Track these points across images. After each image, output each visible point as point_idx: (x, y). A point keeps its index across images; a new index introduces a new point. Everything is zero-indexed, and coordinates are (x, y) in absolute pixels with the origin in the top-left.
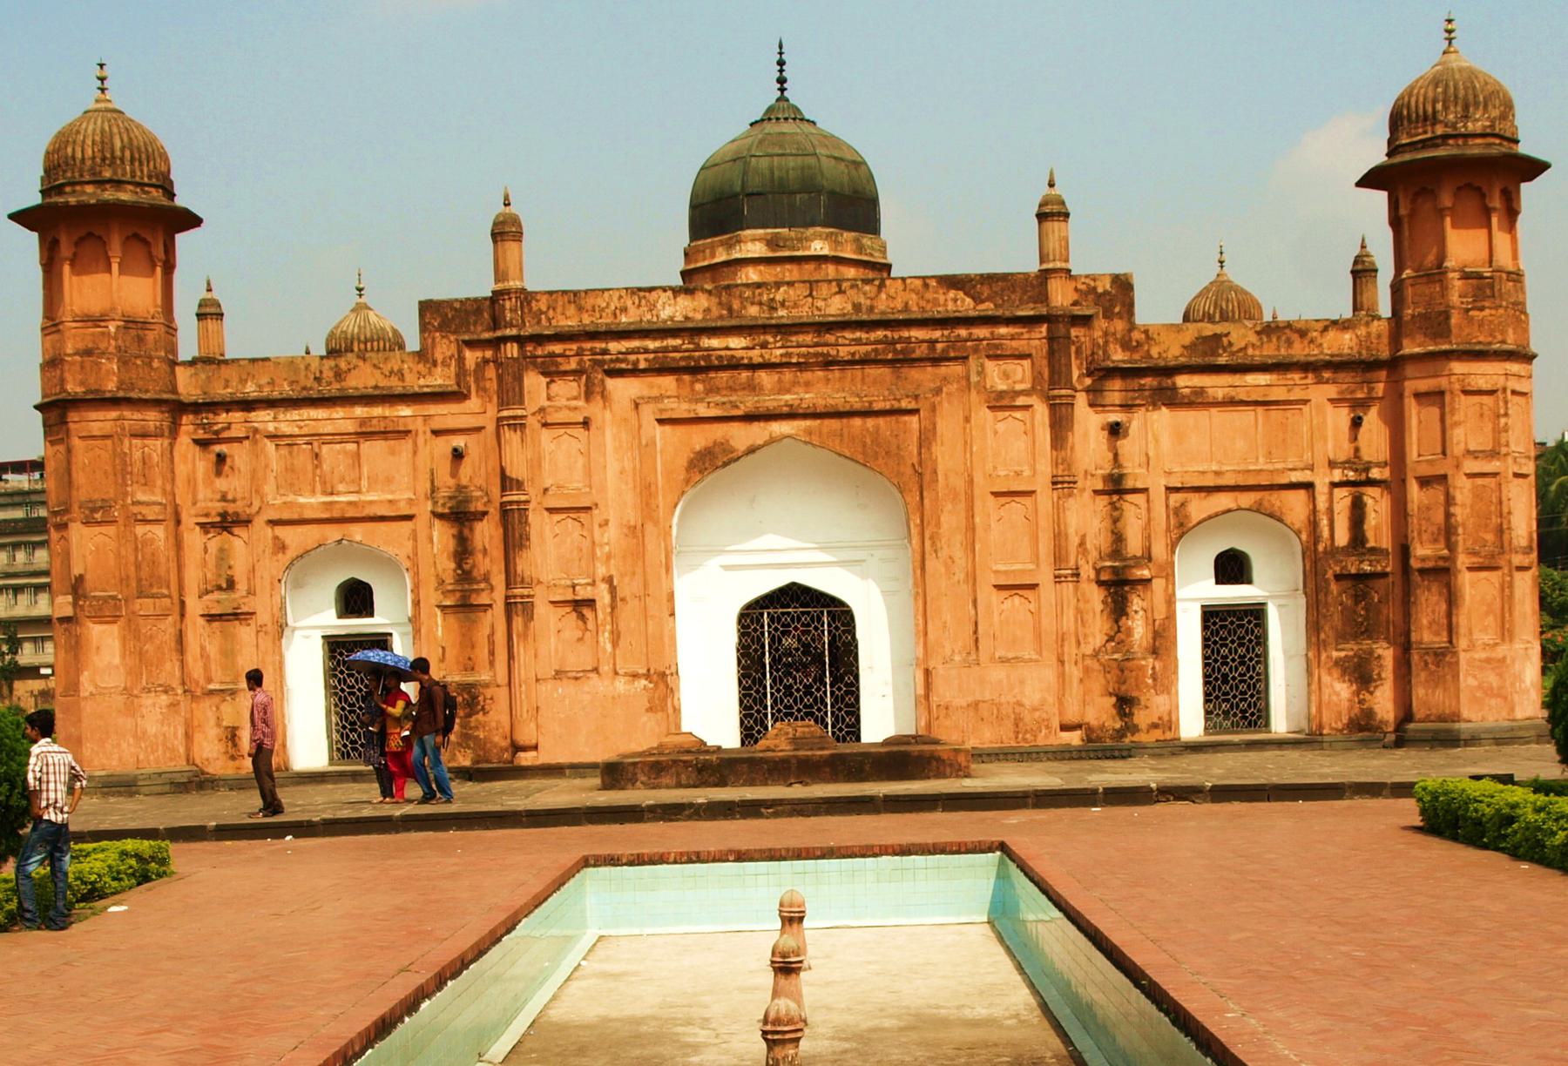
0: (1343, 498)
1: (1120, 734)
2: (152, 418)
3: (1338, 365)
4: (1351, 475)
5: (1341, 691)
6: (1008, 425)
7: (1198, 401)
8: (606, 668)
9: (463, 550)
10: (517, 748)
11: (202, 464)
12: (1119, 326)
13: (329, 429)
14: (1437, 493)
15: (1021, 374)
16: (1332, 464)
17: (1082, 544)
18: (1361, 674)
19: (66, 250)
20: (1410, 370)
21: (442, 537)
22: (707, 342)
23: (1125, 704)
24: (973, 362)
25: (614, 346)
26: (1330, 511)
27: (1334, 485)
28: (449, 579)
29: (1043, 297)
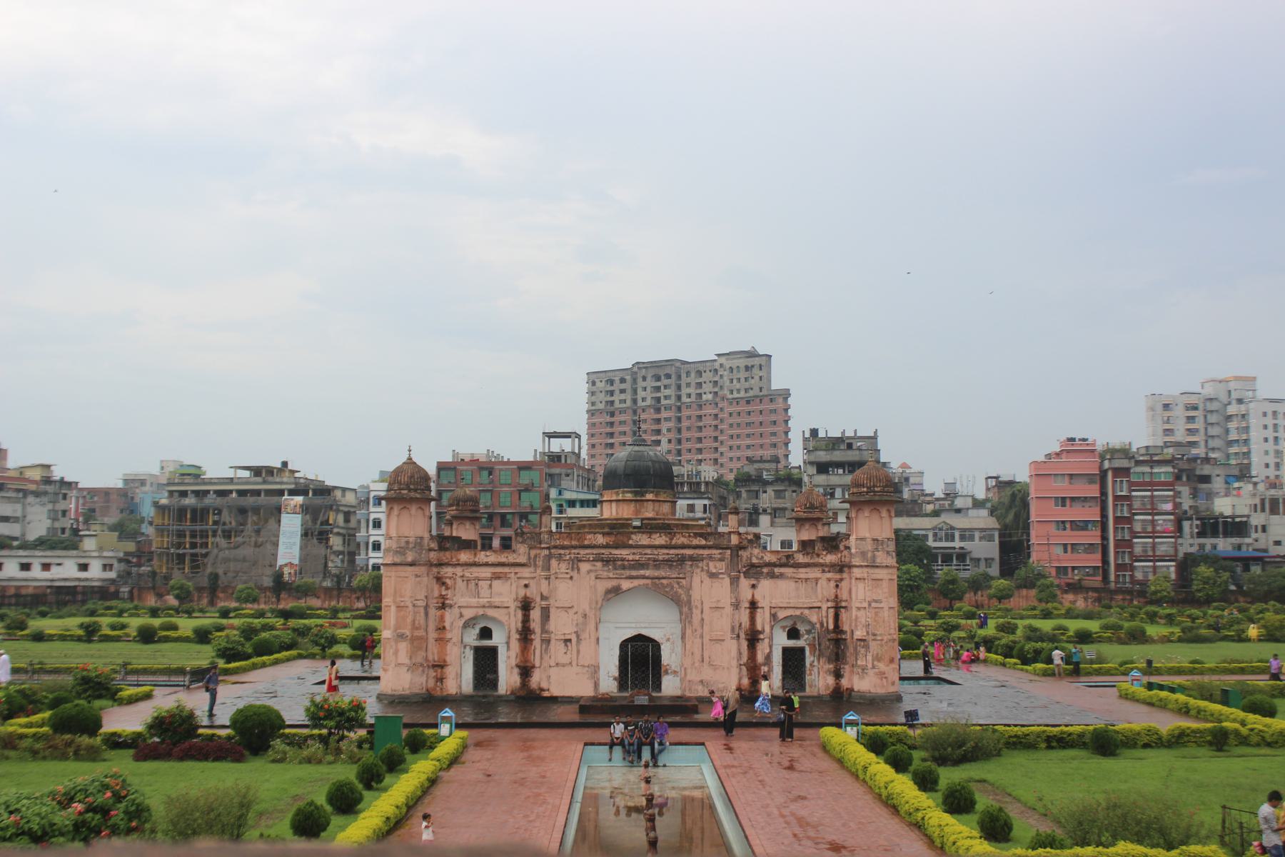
0: (832, 612)
5: (831, 680)
6: (716, 583)
7: (781, 576)
8: (574, 663)
9: (526, 620)
10: (542, 690)
12: (756, 551)
13: (483, 575)
14: (862, 612)
15: (721, 567)
18: (838, 675)
19: (396, 511)
20: (855, 570)
25: (583, 552)
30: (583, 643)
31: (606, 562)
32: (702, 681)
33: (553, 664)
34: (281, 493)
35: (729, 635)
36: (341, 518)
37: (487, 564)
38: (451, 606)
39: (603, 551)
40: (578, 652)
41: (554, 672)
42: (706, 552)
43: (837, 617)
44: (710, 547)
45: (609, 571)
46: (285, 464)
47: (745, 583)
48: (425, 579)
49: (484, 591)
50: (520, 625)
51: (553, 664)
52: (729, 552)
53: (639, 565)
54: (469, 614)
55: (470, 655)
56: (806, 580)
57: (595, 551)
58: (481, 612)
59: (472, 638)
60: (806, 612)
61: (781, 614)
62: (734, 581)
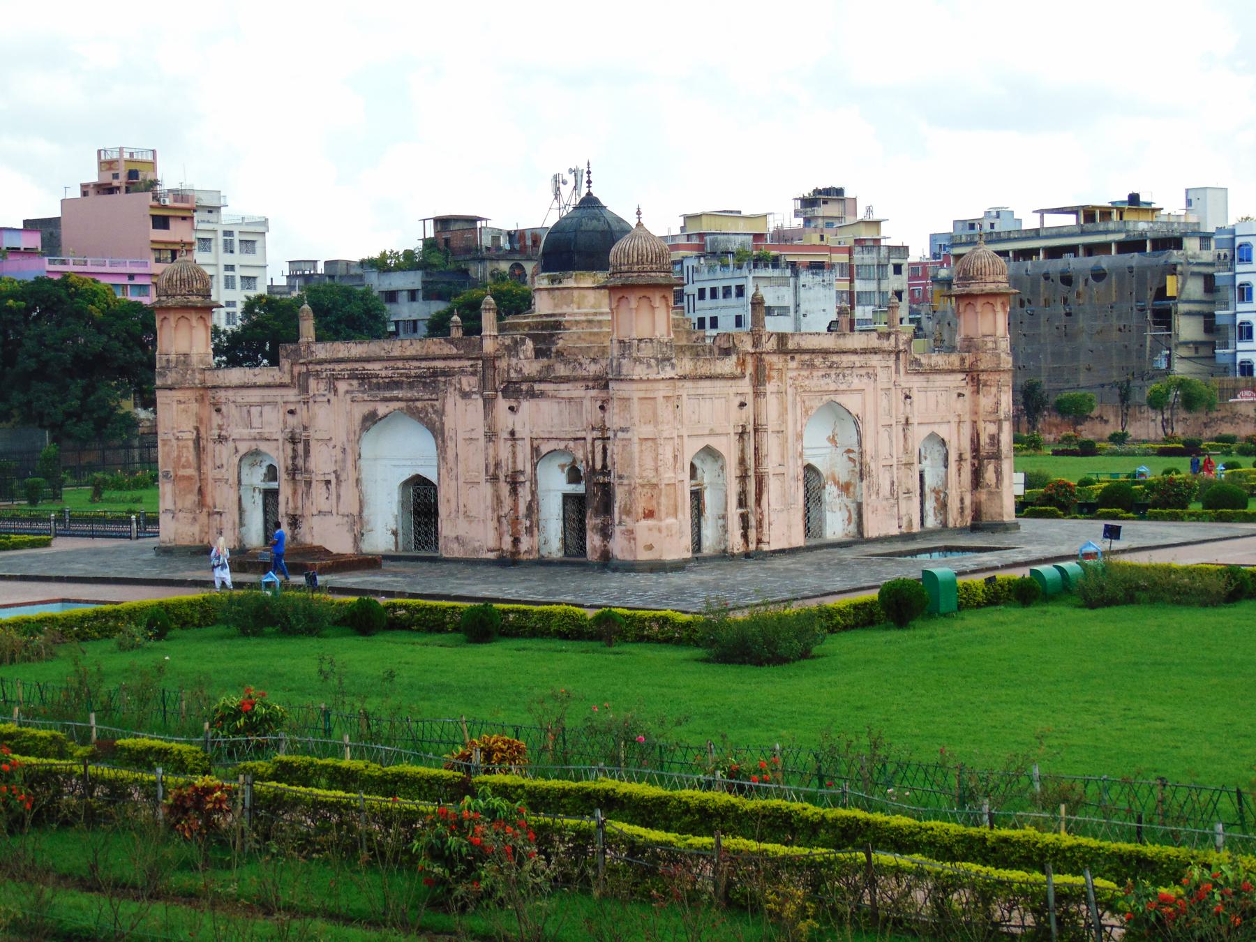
1: (513, 554)
2: (189, 393)
3: (596, 379)
4: (599, 434)
7: (542, 395)
11: (215, 413)
12: (514, 361)
13: (253, 399)
16: (593, 429)
17: (497, 465)
21: (289, 447)
22: (369, 366)
23: (516, 541)
24: (457, 377)
26: (593, 452)
27: (594, 440)
28: (291, 467)
29: (481, 348)
30: (343, 484)
31: (364, 378)
32: (457, 538)
33: (315, 512)
34: (1104, 248)
35: (483, 477)
36: (1195, 288)
37: (255, 386)
38: (226, 439)
39: (356, 365)
40: (339, 497)
41: (316, 522)
42: (456, 364)
43: (605, 450)
44: (460, 358)
45: (364, 392)
46: (1134, 199)
47: (502, 404)
48: (194, 407)
49: (256, 422)
50: (290, 462)
51: (315, 512)
52: (480, 362)
53: (393, 384)
54: (244, 448)
55: (259, 499)
56: (570, 399)
57: (349, 366)
58: (253, 445)
59: (255, 477)
60: (571, 444)
61: (545, 448)
62: (488, 403)
